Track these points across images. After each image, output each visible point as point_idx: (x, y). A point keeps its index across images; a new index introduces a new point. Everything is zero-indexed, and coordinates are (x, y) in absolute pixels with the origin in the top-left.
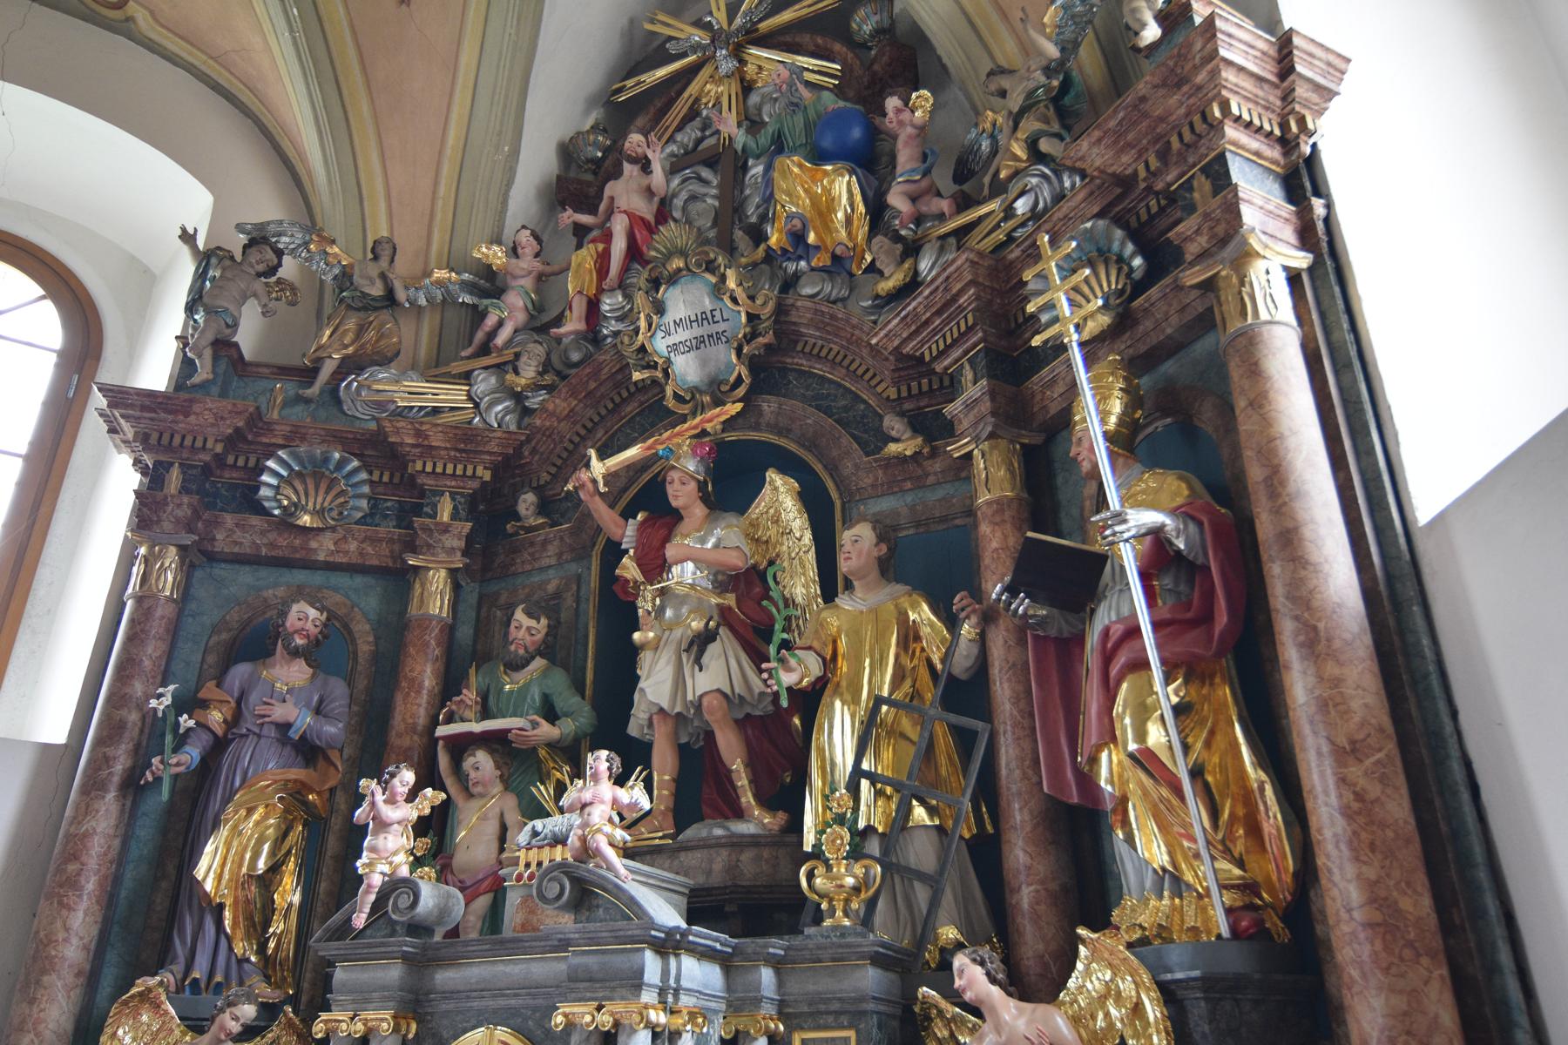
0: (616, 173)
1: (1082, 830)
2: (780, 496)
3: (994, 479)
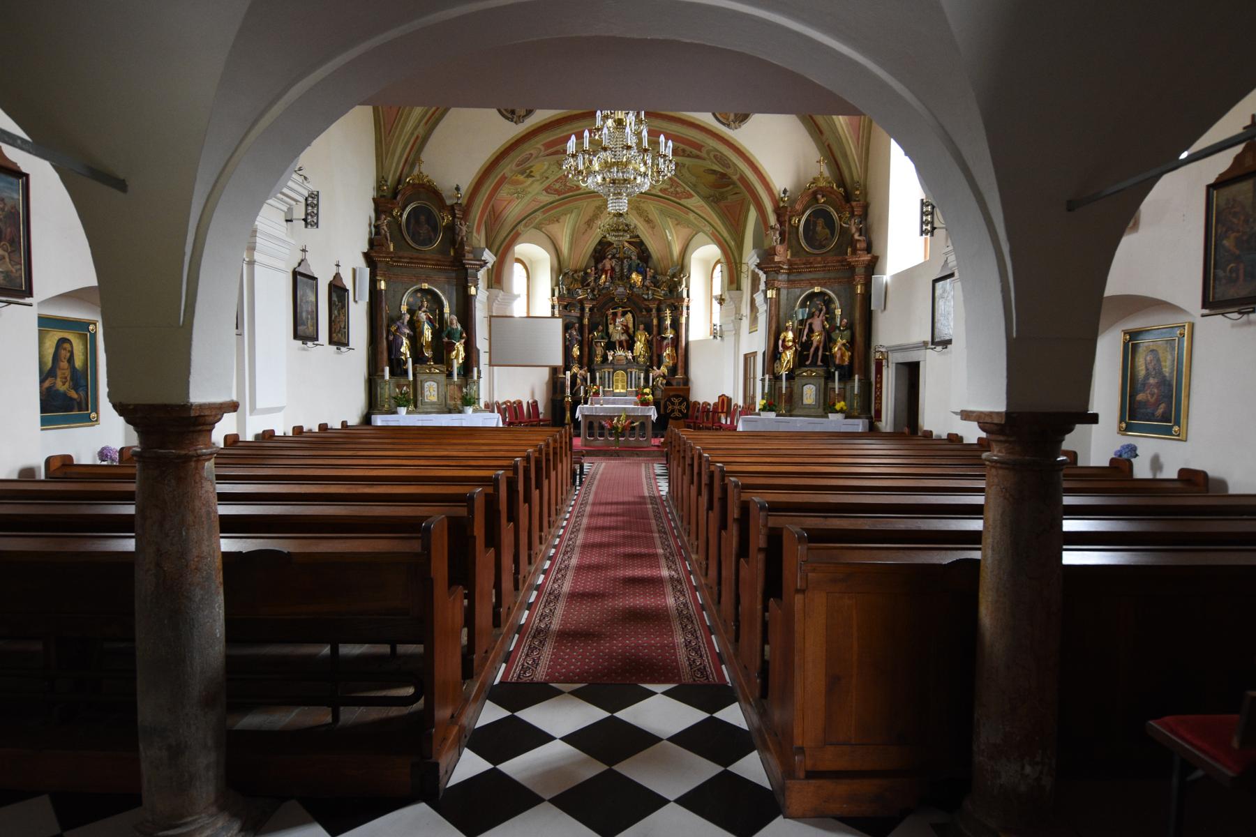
0: (605, 258)
1: (660, 357)
2: (629, 316)
3: (655, 322)
